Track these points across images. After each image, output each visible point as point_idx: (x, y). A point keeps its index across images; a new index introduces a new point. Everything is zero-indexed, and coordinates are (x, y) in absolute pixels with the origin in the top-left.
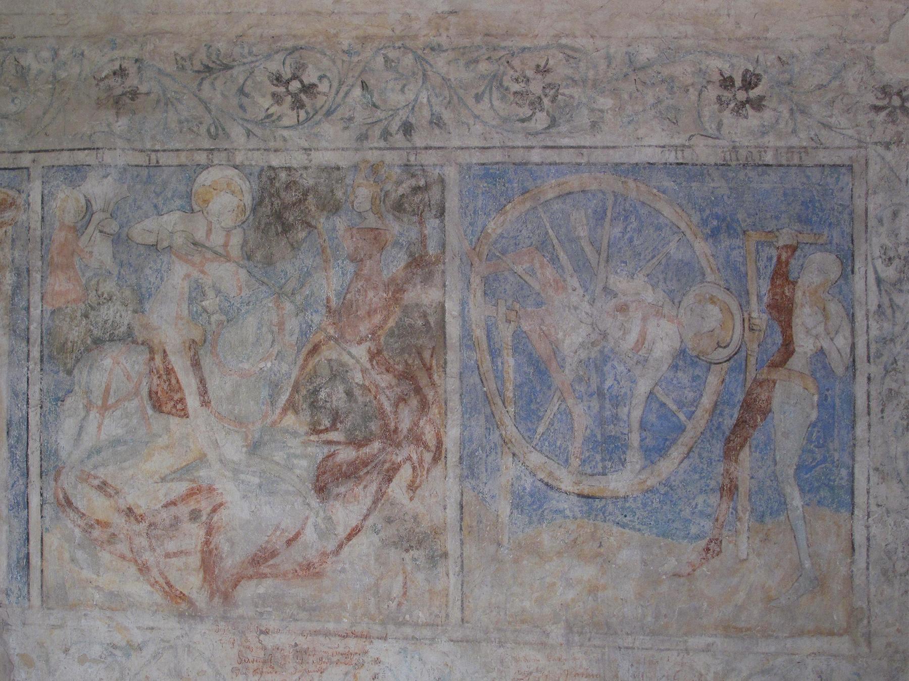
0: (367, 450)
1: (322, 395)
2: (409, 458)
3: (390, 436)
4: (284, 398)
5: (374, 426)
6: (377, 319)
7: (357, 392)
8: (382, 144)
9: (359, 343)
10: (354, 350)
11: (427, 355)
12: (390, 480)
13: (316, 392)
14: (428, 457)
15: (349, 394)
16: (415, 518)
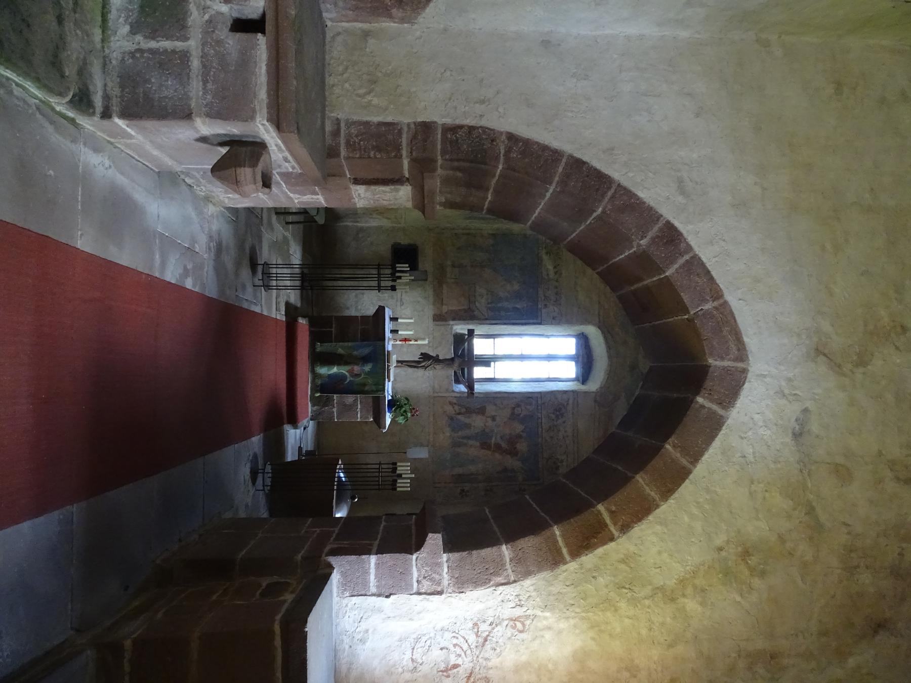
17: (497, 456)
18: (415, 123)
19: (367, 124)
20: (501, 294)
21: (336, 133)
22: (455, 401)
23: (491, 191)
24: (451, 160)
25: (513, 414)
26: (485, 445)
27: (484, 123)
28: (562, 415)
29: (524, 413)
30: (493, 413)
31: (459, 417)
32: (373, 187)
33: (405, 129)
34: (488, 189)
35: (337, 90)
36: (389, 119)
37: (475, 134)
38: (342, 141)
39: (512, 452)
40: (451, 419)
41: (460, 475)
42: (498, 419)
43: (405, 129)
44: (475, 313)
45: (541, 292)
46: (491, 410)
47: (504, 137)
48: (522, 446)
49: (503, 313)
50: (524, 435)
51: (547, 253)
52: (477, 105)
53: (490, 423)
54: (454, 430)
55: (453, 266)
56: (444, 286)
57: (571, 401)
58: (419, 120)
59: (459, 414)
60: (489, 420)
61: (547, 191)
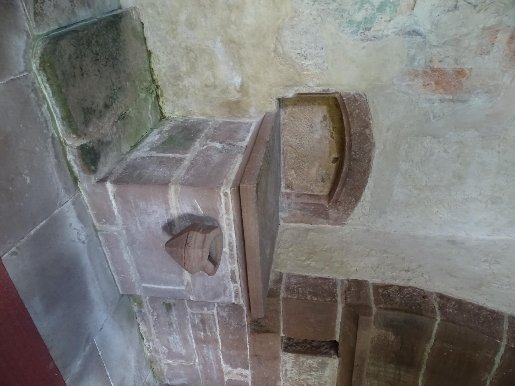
18: (348, 280)
19: (306, 277)
21: (279, 281)
23: (423, 371)
24: (386, 309)
27: (412, 284)
32: (302, 358)
33: (339, 283)
34: (419, 368)
35: (282, 257)
36: (325, 276)
37: (405, 292)
38: (283, 287)
43: (339, 283)
47: (434, 296)
52: (404, 272)
58: (351, 278)
61: (496, 353)
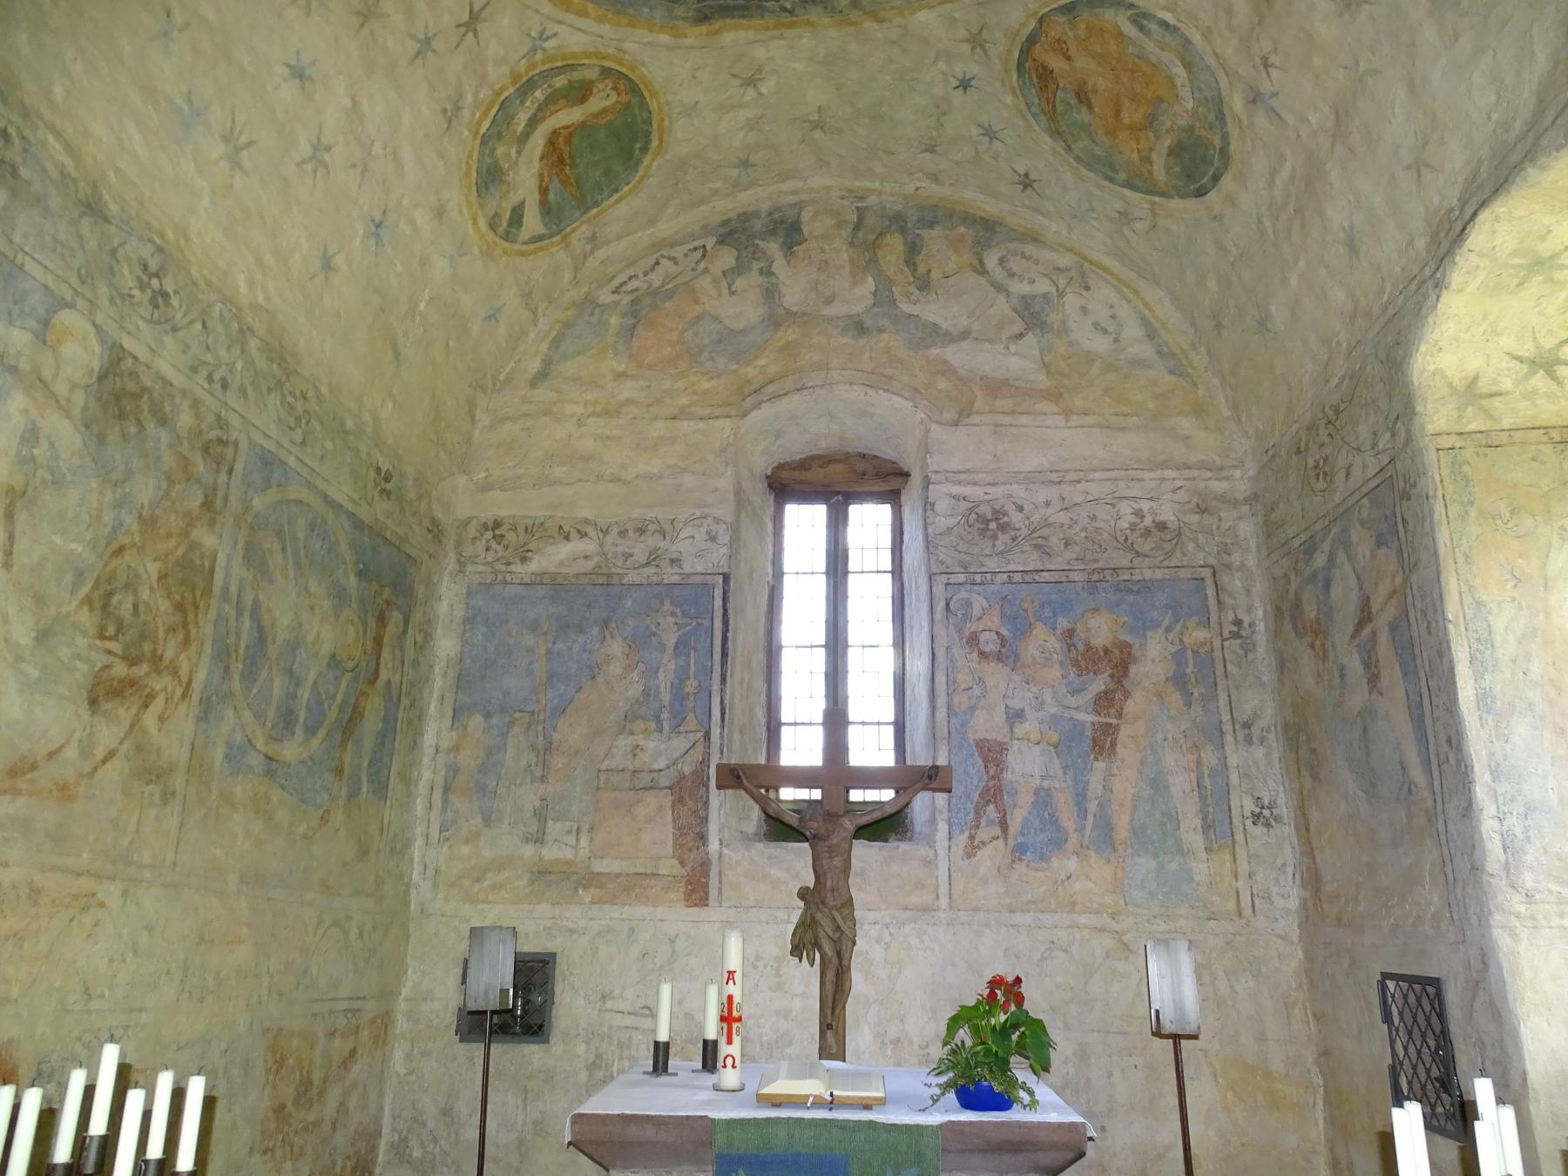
0: (135, 670)
1: (115, 600)
2: (165, 689)
3: (156, 659)
4: (85, 590)
5: (147, 647)
6: (172, 543)
7: (142, 608)
8: (206, 385)
9: (155, 560)
10: (149, 565)
11: (198, 593)
12: (147, 706)
13: (110, 594)
14: (179, 691)
15: (135, 607)
16: (159, 750)
17: (1130, 707)
20: (635, 690)
22: (962, 839)
25: (999, 658)
26: (1103, 742)
28: (998, 514)
29: (994, 621)
30: (999, 717)
31: (1016, 821)
39: (1120, 661)
40: (1020, 851)
41: (1207, 827)
42: (1015, 704)
44: (687, 769)
45: (633, 577)
46: (989, 724)
48: (1100, 630)
49: (691, 686)
50: (1063, 623)
51: (524, 560)
53: (1029, 727)
54: (1058, 843)
55: (539, 839)
56: (599, 866)
57: (957, 490)
59: (1004, 825)
60: (1020, 730)
